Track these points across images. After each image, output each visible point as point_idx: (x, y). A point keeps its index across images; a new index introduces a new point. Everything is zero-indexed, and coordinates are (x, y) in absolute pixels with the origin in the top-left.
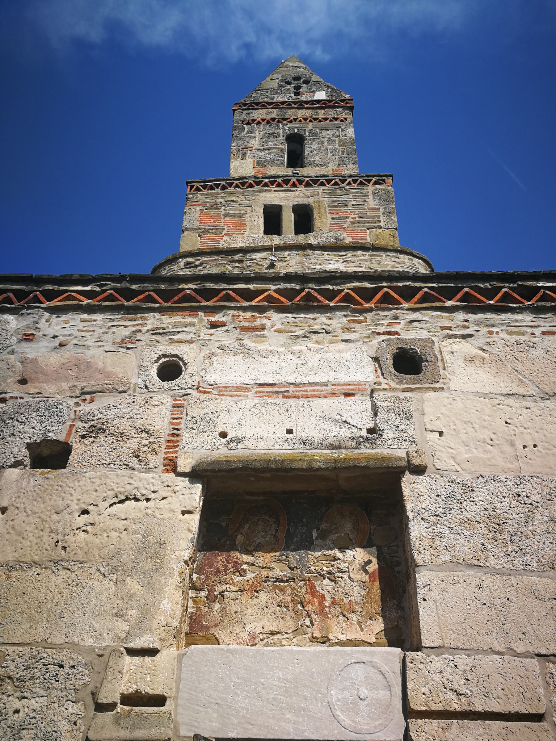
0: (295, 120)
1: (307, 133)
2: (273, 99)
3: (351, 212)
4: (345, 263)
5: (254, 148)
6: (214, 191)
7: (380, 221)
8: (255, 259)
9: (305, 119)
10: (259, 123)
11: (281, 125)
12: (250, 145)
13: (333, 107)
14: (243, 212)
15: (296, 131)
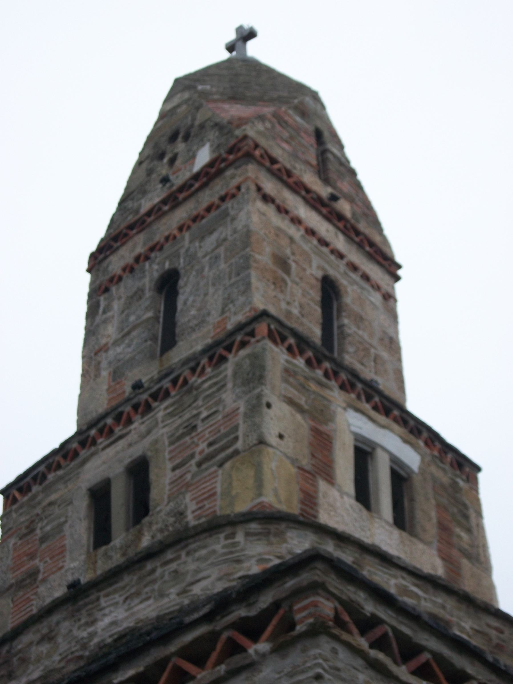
0: (167, 239)
1: (182, 261)
2: (137, 211)
3: (199, 439)
4: (128, 602)
5: (111, 341)
6: (30, 495)
7: (236, 438)
8: (20, 651)
9: (181, 229)
10: (120, 279)
11: (147, 264)
12: (103, 341)
13: (220, 172)
14: (63, 519)
15: (167, 266)
